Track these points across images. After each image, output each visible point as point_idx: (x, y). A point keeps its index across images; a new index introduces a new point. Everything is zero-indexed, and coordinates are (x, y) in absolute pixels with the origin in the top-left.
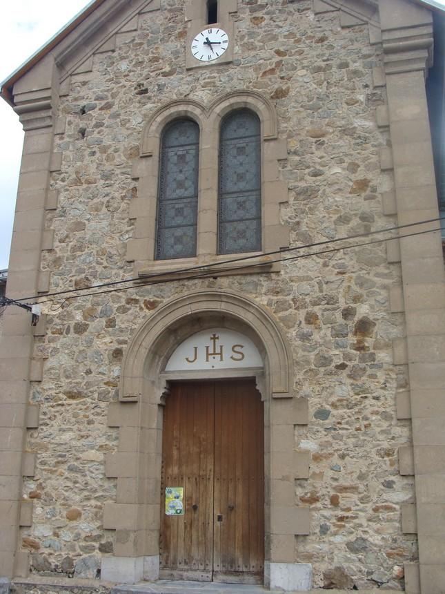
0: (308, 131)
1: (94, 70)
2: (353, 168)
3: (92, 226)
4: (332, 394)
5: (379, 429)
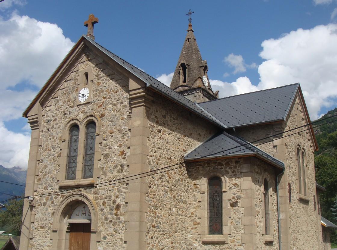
0: (109, 131)
1: (52, 105)
2: (120, 146)
3: (49, 166)
4: (108, 231)
5: (119, 244)
